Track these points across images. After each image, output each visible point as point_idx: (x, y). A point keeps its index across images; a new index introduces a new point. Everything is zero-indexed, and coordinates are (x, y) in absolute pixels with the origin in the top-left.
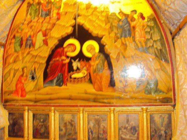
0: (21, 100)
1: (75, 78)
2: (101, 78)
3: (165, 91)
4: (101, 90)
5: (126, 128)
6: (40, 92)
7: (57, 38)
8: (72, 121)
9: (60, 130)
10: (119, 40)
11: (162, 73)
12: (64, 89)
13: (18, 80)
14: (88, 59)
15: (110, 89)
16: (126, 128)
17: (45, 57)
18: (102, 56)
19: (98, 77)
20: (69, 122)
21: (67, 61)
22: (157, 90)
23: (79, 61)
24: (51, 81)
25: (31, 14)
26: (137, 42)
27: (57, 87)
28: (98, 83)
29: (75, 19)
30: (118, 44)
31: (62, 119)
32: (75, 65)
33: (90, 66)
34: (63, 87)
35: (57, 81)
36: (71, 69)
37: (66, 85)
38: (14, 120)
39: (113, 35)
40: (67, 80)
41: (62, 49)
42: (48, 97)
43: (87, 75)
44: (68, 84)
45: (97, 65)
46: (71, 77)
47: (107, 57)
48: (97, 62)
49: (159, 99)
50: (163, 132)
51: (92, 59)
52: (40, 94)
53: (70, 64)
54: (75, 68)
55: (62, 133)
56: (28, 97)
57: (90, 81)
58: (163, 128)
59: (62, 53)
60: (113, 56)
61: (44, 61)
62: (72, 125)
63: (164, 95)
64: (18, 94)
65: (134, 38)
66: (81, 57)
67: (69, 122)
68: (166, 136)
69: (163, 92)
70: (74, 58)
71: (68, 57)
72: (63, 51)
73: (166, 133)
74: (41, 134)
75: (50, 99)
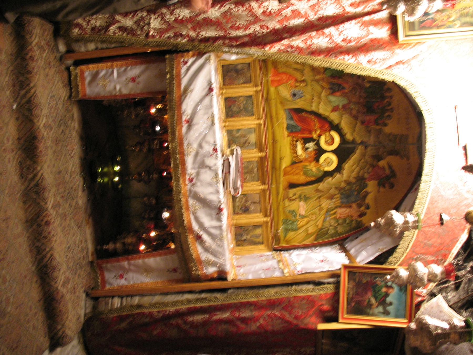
0: (267, 81)
1: (296, 146)
2: (297, 174)
3: (286, 238)
4: (285, 174)
5: (246, 201)
6: (279, 105)
7: (339, 123)
8: (249, 143)
9: (238, 130)
10: (337, 192)
11: (303, 235)
12: (284, 133)
13: (290, 76)
14: (317, 159)
15: (286, 184)
16: (246, 201)
17: (319, 109)
18: (321, 174)
19: (298, 171)
20: (247, 140)
21: (315, 136)
22: (287, 231)
23: (315, 150)
24: (291, 118)
25: (370, 87)
26: (335, 211)
27: (285, 126)
28: (292, 172)
29: (362, 143)
30: (333, 191)
31: (249, 131)
32: (311, 145)
33: (310, 162)
34: (286, 133)
35: (292, 126)
36: (306, 140)
37: (288, 136)
38: (242, 70)
39: (343, 185)
40: (294, 137)
41: (328, 129)
42: (274, 116)
43: (299, 159)
44: (289, 139)
45: (311, 170)
46: (297, 141)
47: (319, 180)
48: (314, 169)
49: (278, 233)
50: (244, 237)
51: (316, 164)
52: (276, 104)
53: (311, 140)
54: (307, 145)
55: (234, 133)
56: (272, 89)
57: (294, 163)
58: (249, 237)
59: (323, 131)
60: (321, 186)
61: (314, 108)
62: (245, 143)
63: (282, 238)
64: (273, 76)
65: (340, 207)
66: (320, 152)
67: (247, 140)
68: (241, 241)
69: (285, 237)
70: (318, 144)
71: (319, 136)
72: (326, 131)
73: (245, 240)
74: (230, 107)
75: (271, 118)
